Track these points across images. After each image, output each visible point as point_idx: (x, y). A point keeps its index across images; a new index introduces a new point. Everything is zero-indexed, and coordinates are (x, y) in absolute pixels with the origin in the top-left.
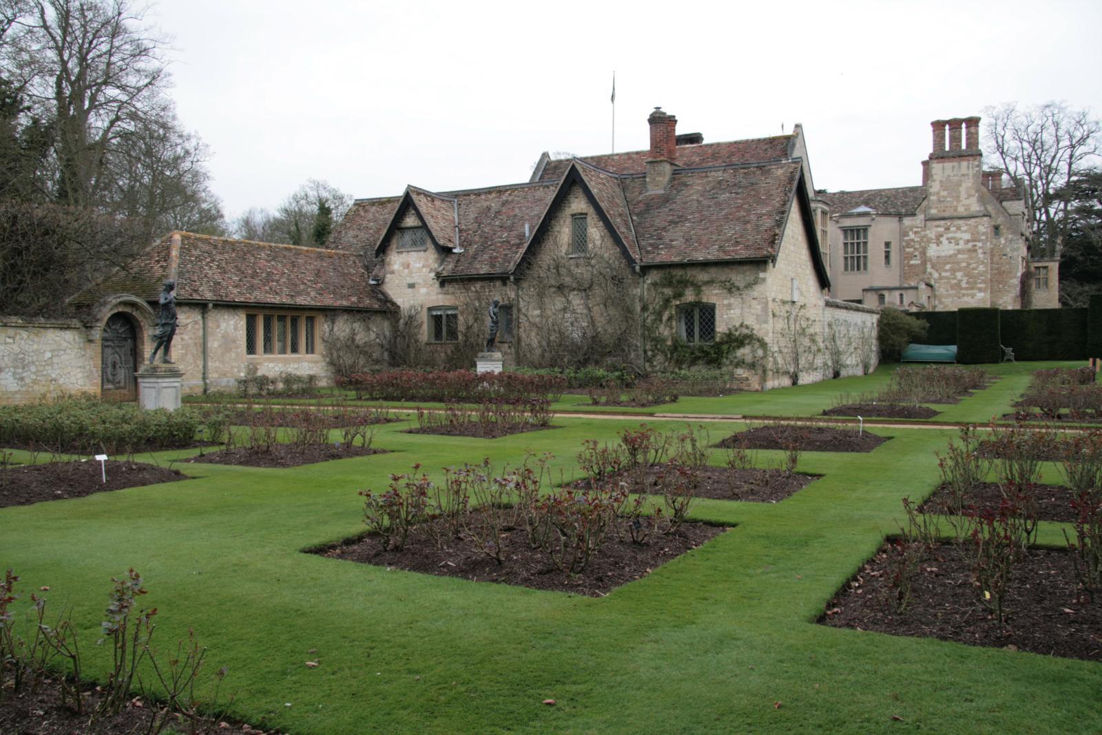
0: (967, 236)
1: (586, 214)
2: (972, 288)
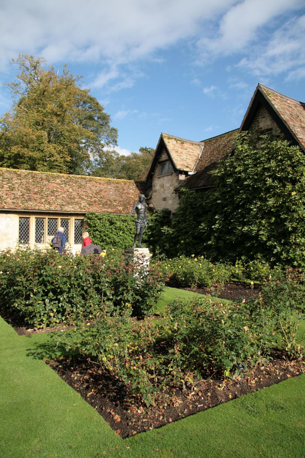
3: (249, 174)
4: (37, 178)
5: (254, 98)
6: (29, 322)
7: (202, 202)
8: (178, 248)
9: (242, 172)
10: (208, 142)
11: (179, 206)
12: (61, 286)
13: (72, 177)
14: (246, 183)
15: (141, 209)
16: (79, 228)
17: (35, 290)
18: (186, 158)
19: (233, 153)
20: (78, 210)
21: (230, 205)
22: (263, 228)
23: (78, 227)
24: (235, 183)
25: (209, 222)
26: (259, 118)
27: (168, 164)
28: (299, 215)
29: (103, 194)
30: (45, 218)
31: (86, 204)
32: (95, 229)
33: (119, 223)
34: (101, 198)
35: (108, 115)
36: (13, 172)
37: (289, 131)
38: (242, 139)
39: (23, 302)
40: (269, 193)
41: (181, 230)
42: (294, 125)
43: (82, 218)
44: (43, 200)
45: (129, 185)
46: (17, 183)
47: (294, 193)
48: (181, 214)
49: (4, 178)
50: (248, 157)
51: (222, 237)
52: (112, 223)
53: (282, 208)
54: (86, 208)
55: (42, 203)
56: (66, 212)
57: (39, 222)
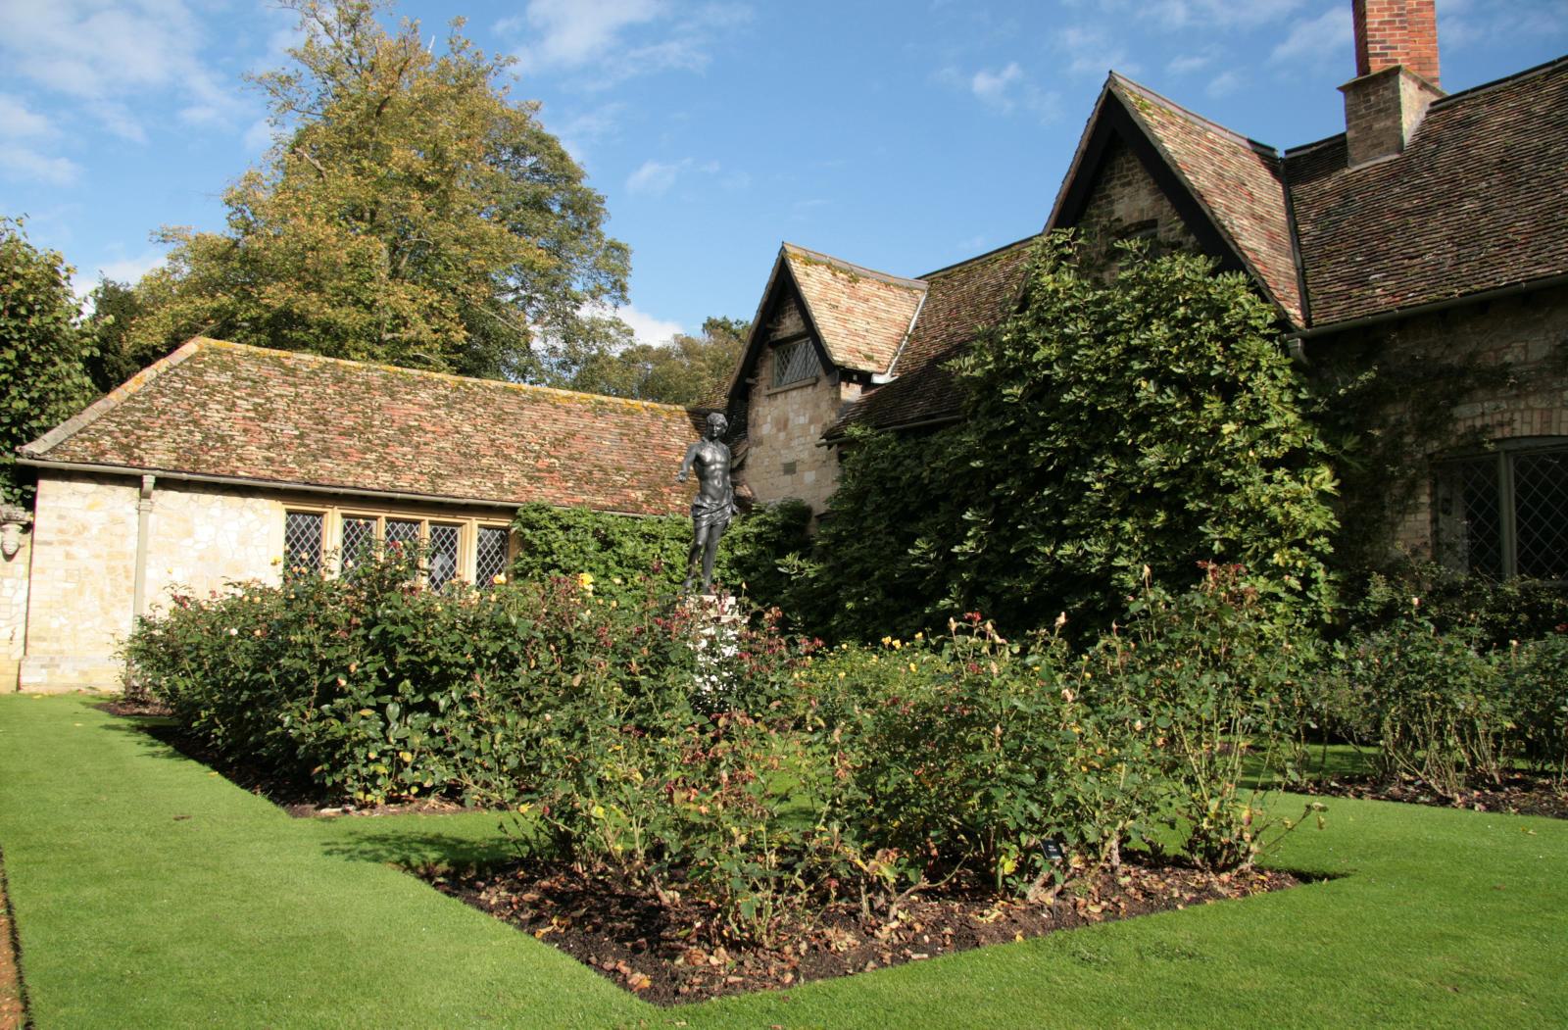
3: (1081, 369)
4: (351, 383)
5: (1095, 119)
6: (329, 782)
7: (918, 470)
8: (836, 626)
9: (1056, 361)
10: (939, 280)
11: (838, 486)
12: (446, 655)
13: (474, 384)
14: (1067, 397)
15: (714, 462)
16: (492, 559)
17: (353, 668)
18: (867, 327)
19: (1024, 304)
20: (489, 493)
21: (1013, 475)
22: (1126, 548)
23: (489, 552)
24: (1031, 399)
25: (941, 534)
26: (1113, 188)
27: (803, 347)
28: (1247, 500)
29: (577, 446)
30: (375, 518)
31: (518, 474)
32: (548, 560)
33: (631, 544)
34: (571, 457)
35: (598, 197)
36: (271, 358)
37: (1213, 226)
38: (1055, 254)
39: (311, 714)
40: (1146, 431)
41: (845, 565)
42: (1227, 207)
43: (504, 523)
44: (371, 457)
45: (669, 420)
46: (281, 396)
47: (1228, 428)
48: (846, 513)
49: (238, 379)
50: (1074, 315)
51: (986, 583)
52: (606, 544)
53: (1190, 481)
54: (518, 490)
55: (368, 466)
56: (449, 500)
57: (353, 530)
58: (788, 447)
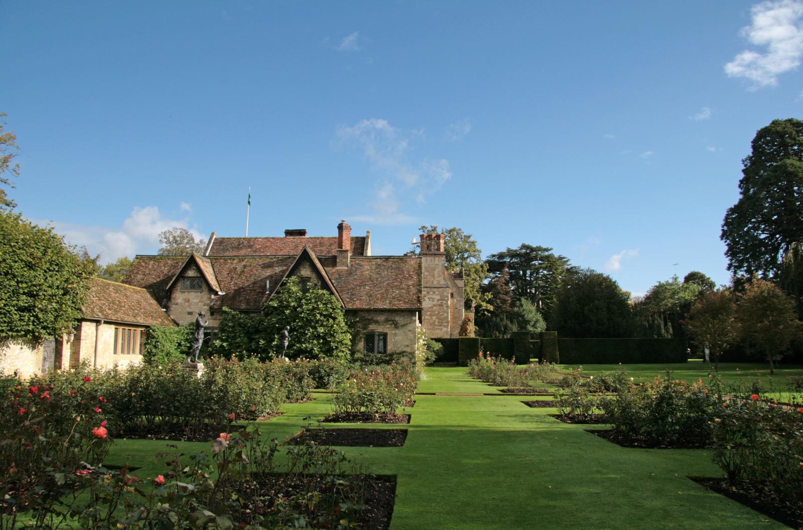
0: (438, 297)
1: (310, 278)
2: (441, 326)
58: (190, 307)
